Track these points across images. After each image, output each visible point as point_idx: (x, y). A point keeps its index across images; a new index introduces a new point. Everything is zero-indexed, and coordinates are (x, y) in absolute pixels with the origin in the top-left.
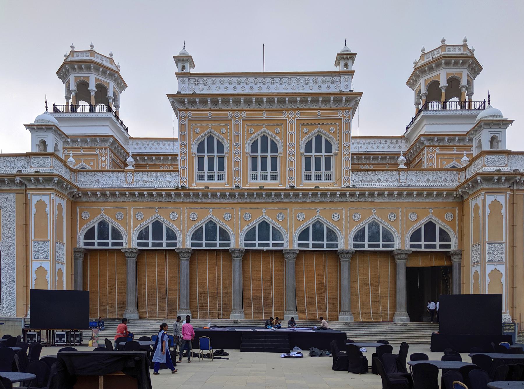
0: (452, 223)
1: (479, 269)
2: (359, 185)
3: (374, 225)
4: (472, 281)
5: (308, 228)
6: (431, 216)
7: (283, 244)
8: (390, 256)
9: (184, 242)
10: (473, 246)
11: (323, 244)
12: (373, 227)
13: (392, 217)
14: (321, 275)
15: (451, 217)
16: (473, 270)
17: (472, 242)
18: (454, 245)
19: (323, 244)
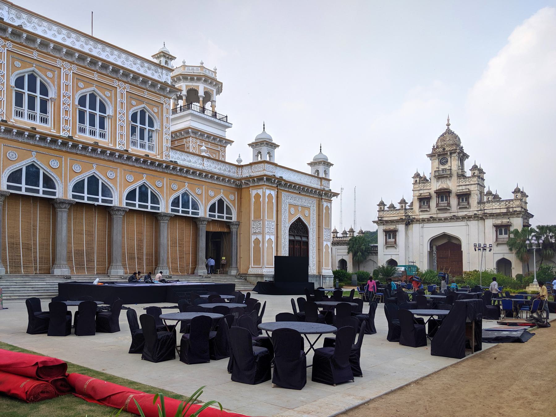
0: (233, 202)
1: (260, 237)
2: (180, 162)
3: (185, 195)
4: (252, 245)
5: (135, 190)
6: (222, 195)
7: (112, 201)
8: (194, 222)
9: (65, 192)
10: (254, 221)
11: (148, 206)
12: (185, 197)
13: (199, 191)
14: (140, 233)
15: (233, 198)
16: (253, 238)
17: (252, 218)
18: (234, 219)
19: (148, 206)
